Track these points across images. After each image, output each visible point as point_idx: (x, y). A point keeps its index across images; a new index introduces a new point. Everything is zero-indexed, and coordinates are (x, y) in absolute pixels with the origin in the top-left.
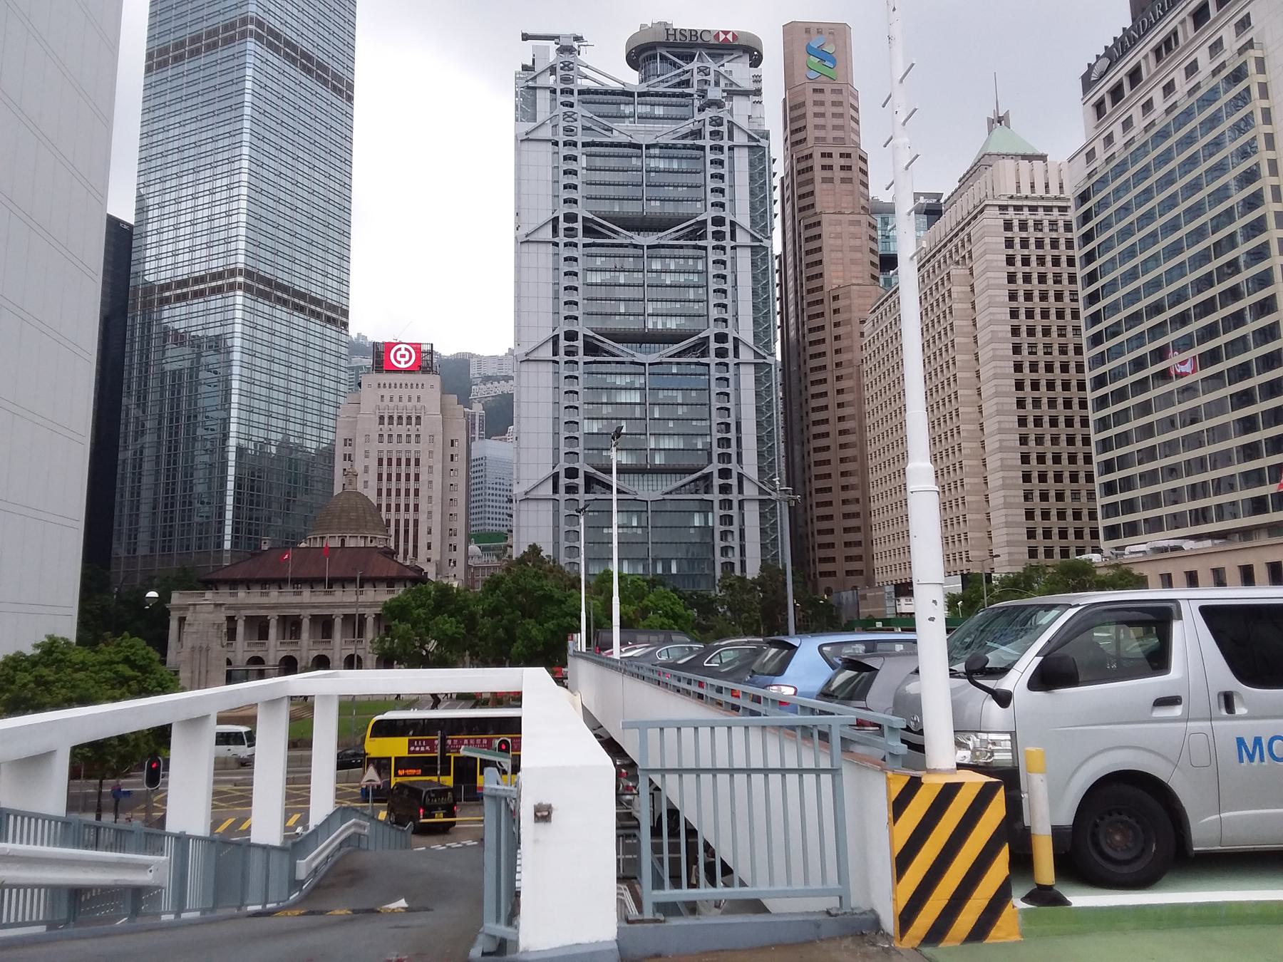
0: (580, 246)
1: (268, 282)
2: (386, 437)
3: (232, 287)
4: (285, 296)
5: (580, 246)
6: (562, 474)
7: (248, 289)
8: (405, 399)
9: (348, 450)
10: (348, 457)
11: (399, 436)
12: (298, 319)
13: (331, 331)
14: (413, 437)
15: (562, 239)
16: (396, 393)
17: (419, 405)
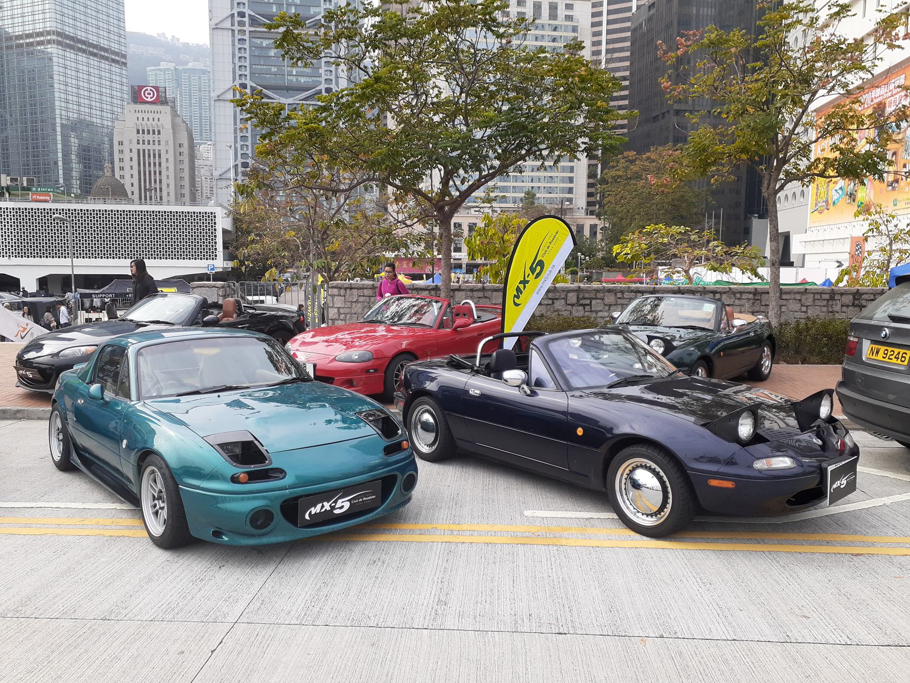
0: (247, 33)
1: (72, 38)
2: (141, 142)
3: (49, 42)
4: (84, 47)
5: (247, 33)
6: (240, 165)
7: (59, 43)
8: (151, 119)
9: (121, 147)
10: (121, 152)
11: (149, 141)
12: (94, 61)
13: (115, 68)
14: (156, 142)
15: (236, 28)
16: (146, 116)
17: (159, 123)
